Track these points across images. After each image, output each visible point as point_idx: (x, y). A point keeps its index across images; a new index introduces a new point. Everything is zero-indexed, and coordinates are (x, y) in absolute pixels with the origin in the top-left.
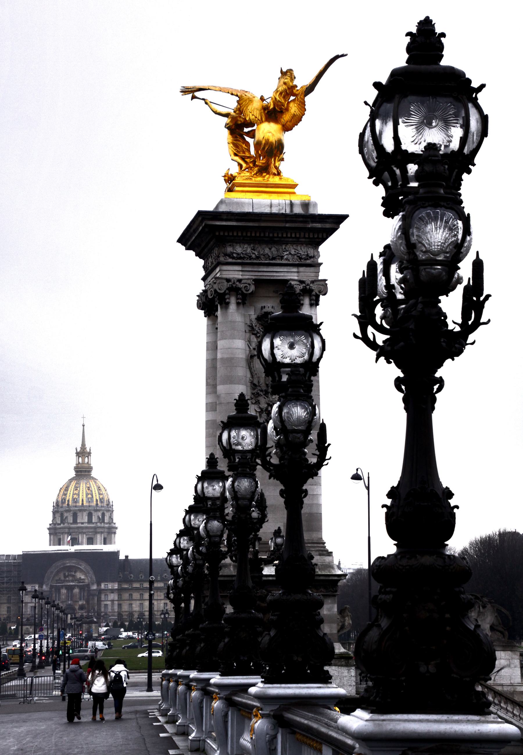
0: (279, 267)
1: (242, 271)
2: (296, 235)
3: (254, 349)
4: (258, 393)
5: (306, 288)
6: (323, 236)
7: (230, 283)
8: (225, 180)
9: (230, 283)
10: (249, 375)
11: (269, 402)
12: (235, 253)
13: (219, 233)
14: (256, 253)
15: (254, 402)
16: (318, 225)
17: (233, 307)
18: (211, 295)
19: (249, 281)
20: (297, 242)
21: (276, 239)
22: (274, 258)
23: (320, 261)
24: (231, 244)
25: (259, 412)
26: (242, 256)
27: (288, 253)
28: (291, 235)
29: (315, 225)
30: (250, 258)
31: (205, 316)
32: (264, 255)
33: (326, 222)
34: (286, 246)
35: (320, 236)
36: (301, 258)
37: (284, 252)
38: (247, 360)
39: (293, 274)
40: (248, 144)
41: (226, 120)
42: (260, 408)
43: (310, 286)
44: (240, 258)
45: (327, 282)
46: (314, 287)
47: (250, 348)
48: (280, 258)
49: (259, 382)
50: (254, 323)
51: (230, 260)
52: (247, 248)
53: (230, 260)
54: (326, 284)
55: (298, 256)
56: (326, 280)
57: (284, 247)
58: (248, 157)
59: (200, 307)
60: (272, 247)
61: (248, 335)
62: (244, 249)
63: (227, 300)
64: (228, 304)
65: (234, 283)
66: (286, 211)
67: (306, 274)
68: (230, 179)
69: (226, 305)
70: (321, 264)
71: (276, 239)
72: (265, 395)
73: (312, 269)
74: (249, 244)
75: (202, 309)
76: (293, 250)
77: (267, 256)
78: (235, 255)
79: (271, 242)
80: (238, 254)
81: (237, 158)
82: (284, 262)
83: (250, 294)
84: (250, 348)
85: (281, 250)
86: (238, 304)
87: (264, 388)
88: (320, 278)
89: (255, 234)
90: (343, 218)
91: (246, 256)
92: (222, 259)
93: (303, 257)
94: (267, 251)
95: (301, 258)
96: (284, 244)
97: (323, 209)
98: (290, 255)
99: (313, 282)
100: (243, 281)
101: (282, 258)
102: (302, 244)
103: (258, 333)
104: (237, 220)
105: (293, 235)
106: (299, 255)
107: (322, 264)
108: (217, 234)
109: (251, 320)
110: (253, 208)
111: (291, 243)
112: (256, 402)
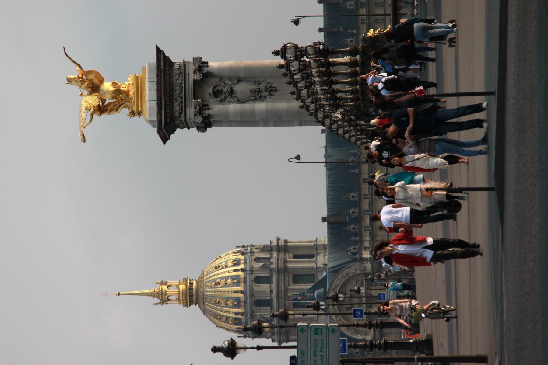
0: (186, 85)
1: (189, 107)
2: (168, 76)
3: (234, 99)
4: (260, 97)
5: (198, 69)
6: (167, 60)
7: (197, 113)
8: (133, 117)
9: (197, 113)
10: (250, 102)
11: (265, 90)
12: (179, 111)
13: (168, 120)
14: (179, 98)
15: (264, 99)
16: (162, 62)
17: (210, 112)
18: (202, 124)
20: (171, 75)
21: (170, 87)
22: (181, 88)
23: (182, 61)
24: (174, 113)
25: (271, 96)
26: (180, 107)
27: (178, 80)
28: (168, 78)
29: (162, 65)
30: (181, 102)
31: (211, 127)
32: (180, 94)
33: (160, 58)
34: (174, 81)
35: (168, 61)
36: (181, 73)
37: (177, 82)
38: (240, 103)
39: (190, 77)
40: (110, 104)
41: (95, 116)
42: (268, 96)
43: (197, 67)
44: (182, 108)
45: (194, 58)
47: (233, 102)
48: (181, 85)
49: (253, 96)
50: (218, 99)
51: (183, 114)
52: (176, 104)
54: (196, 58)
55: (180, 74)
56: (193, 59)
57: (174, 83)
58: (119, 103)
59: (205, 130)
60: (175, 90)
61: (225, 103)
62: (177, 105)
64: (209, 115)
67: (191, 69)
68: (133, 113)
69: (209, 116)
71: (170, 87)
72: (260, 93)
73: (187, 66)
74: (174, 103)
75: (206, 129)
76: (176, 77)
77: (180, 92)
78: (180, 111)
79: (172, 90)
80: (180, 109)
81: (119, 110)
82: (183, 82)
84: (233, 102)
85: (176, 84)
86: (208, 109)
87: (257, 93)
88: (192, 61)
89: (168, 99)
91: (181, 105)
92: (183, 119)
93: (180, 71)
94: (177, 92)
95: (181, 73)
96: (172, 82)
98: (179, 79)
99: (195, 65)
100: (196, 106)
101: (181, 83)
102: (172, 72)
103: (224, 97)
104: (161, 110)
105: (168, 77)
106: (179, 73)
107: (183, 60)
108: (169, 121)
109: (217, 101)
110: (152, 101)
111: (172, 79)
112: (265, 98)
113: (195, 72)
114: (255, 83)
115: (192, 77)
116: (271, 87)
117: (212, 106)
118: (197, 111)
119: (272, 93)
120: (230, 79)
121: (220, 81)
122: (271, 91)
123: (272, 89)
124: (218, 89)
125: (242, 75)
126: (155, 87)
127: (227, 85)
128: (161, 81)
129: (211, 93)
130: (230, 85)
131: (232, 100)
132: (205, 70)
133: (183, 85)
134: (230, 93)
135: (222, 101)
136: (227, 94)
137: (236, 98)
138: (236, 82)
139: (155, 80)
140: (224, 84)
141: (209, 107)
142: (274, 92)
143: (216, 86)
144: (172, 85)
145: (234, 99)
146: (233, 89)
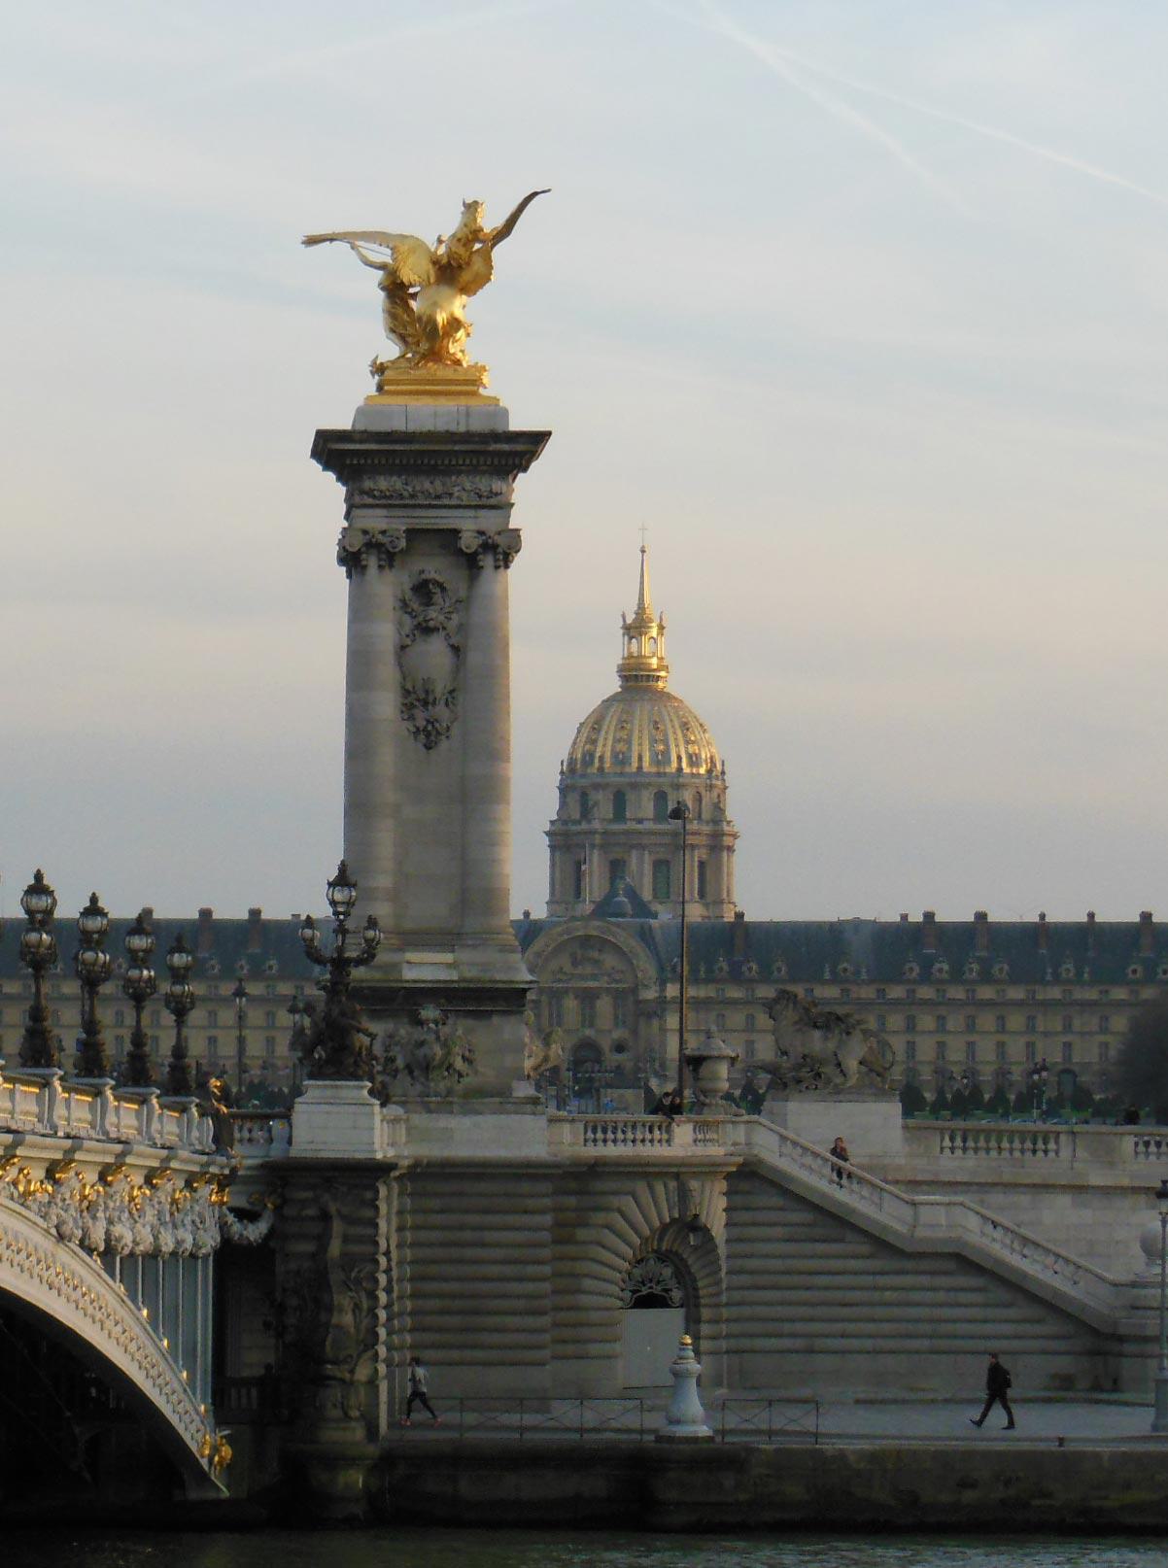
1: (387, 517)
3: (408, 636)
5: (487, 543)
9: (368, 537)
10: (398, 676)
15: (406, 717)
16: (506, 447)
19: (396, 534)
20: (474, 470)
21: (442, 468)
22: (438, 497)
23: (512, 501)
26: (388, 494)
27: (460, 488)
30: (401, 496)
32: (423, 492)
33: (518, 442)
36: (480, 497)
38: (396, 653)
42: (415, 726)
44: (385, 497)
46: (498, 539)
49: (414, 687)
50: (409, 595)
51: (370, 501)
53: (370, 501)
56: (518, 530)
57: (454, 478)
63: (364, 563)
64: (365, 567)
65: (373, 536)
66: (458, 424)
67: (488, 521)
70: (513, 504)
79: (433, 471)
80: (381, 492)
82: (454, 502)
83: (402, 551)
84: (400, 634)
86: (380, 567)
87: (422, 696)
88: (512, 526)
90: (548, 434)
92: (357, 499)
93: (485, 494)
94: (427, 485)
95: (480, 497)
96: (454, 474)
97: (517, 424)
99: (499, 533)
101: (451, 495)
102: (483, 473)
103: (413, 610)
105: (468, 462)
108: (348, 462)
109: (403, 591)
113: (481, 533)
114: (451, 692)
115: (469, 525)
116: (439, 733)
117: (390, 576)
118: (373, 536)
119: (422, 736)
120: (461, 627)
121: (457, 601)
122: (428, 735)
123: (433, 738)
124: (435, 593)
125: (473, 658)
126: (441, 426)
127: (446, 617)
128: (455, 443)
129: (423, 576)
130: (445, 625)
131: (407, 629)
132: (487, 561)
133: (446, 501)
134: (424, 625)
135: (404, 605)
136: (421, 619)
137: (409, 643)
138: (454, 641)
139: (462, 429)
140: (451, 609)
141: (387, 570)
142: (424, 741)
143: (443, 589)
144: (447, 471)
145: (408, 636)
146: (435, 634)
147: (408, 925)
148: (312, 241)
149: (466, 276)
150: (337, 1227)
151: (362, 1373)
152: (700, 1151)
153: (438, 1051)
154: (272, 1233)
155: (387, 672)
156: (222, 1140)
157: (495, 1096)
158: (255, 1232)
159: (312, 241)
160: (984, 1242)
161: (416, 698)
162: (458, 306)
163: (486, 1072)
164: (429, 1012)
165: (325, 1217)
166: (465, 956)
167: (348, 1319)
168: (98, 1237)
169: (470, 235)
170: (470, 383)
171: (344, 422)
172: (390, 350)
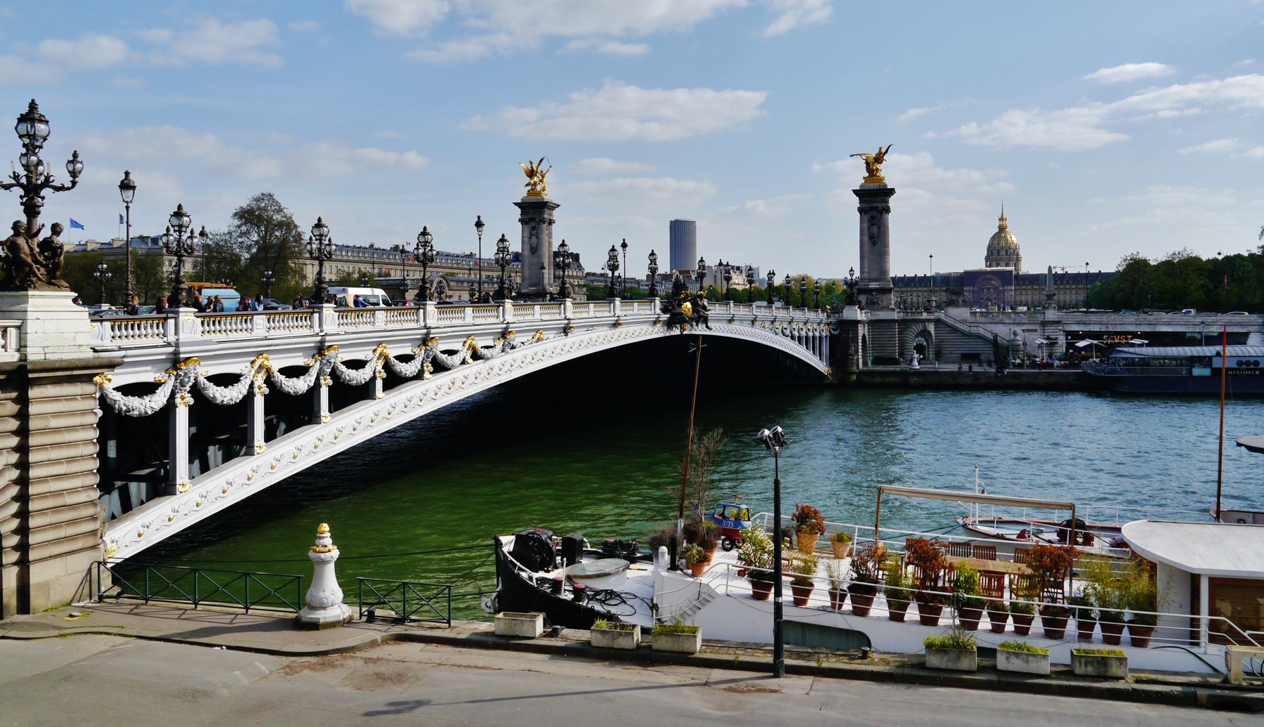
67: (884, 205)
115: (880, 205)
117: (866, 215)
120: (880, 224)
125: (882, 230)
135: (869, 220)
147: (871, 277)
148: (851, 156)
149: (880, 161)
150: (851, 332)
151: (855, 358)
152: (928, 317)
153: (875, 300)
154: (840, 332)
155: (866, 232)
156: (828, 317)
157: (887, 308)
158: (836, 333)
159: (851, 156)
160: (986, 335)
161: (871, 237)
162: (879, 166)
163: (885, 304)
164: (874, 294)
165: (849, 330)
166: (881, 283)
167: (853, 348)
168: (796, 333)
169: (880, 153)
170: (881, 179)
171: (858, 188)
172: (867, 175)
